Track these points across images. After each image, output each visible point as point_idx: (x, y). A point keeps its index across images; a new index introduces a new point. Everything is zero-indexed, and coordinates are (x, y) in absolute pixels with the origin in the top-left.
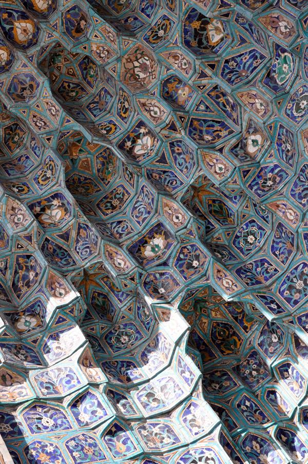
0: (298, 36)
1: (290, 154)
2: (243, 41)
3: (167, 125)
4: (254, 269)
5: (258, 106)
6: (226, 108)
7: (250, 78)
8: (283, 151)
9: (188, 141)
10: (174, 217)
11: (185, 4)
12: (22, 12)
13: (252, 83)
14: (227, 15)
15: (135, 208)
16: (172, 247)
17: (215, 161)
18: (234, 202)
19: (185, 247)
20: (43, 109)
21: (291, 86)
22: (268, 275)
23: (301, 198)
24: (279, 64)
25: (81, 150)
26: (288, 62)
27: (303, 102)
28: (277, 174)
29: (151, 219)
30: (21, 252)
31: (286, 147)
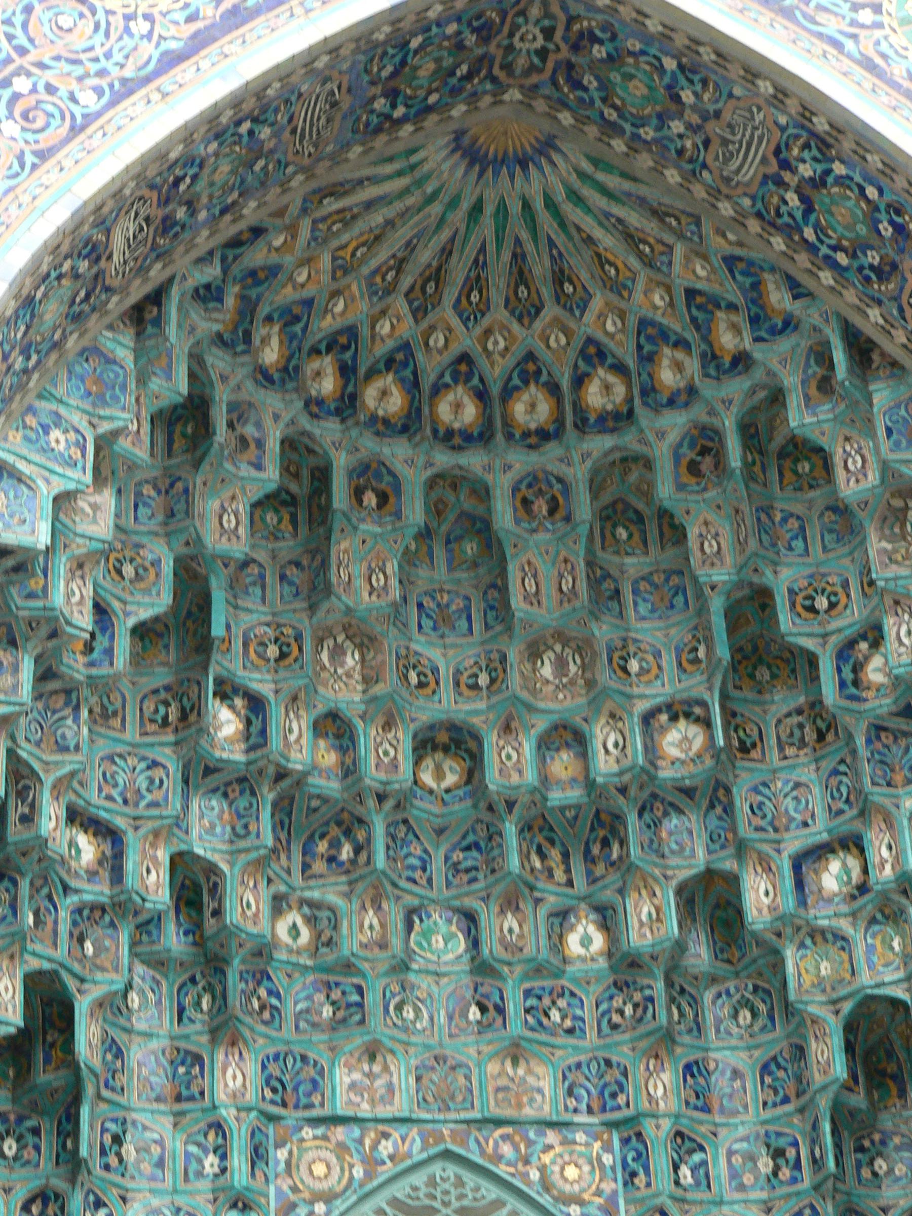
0: (509, 964)
1: (316, 1019)
2: (440, 832)
7: (403, 884)
9: (266, 815)
13: (396, 892)
14: (490, 808)
19: (104, 910)
30: (19, 630)
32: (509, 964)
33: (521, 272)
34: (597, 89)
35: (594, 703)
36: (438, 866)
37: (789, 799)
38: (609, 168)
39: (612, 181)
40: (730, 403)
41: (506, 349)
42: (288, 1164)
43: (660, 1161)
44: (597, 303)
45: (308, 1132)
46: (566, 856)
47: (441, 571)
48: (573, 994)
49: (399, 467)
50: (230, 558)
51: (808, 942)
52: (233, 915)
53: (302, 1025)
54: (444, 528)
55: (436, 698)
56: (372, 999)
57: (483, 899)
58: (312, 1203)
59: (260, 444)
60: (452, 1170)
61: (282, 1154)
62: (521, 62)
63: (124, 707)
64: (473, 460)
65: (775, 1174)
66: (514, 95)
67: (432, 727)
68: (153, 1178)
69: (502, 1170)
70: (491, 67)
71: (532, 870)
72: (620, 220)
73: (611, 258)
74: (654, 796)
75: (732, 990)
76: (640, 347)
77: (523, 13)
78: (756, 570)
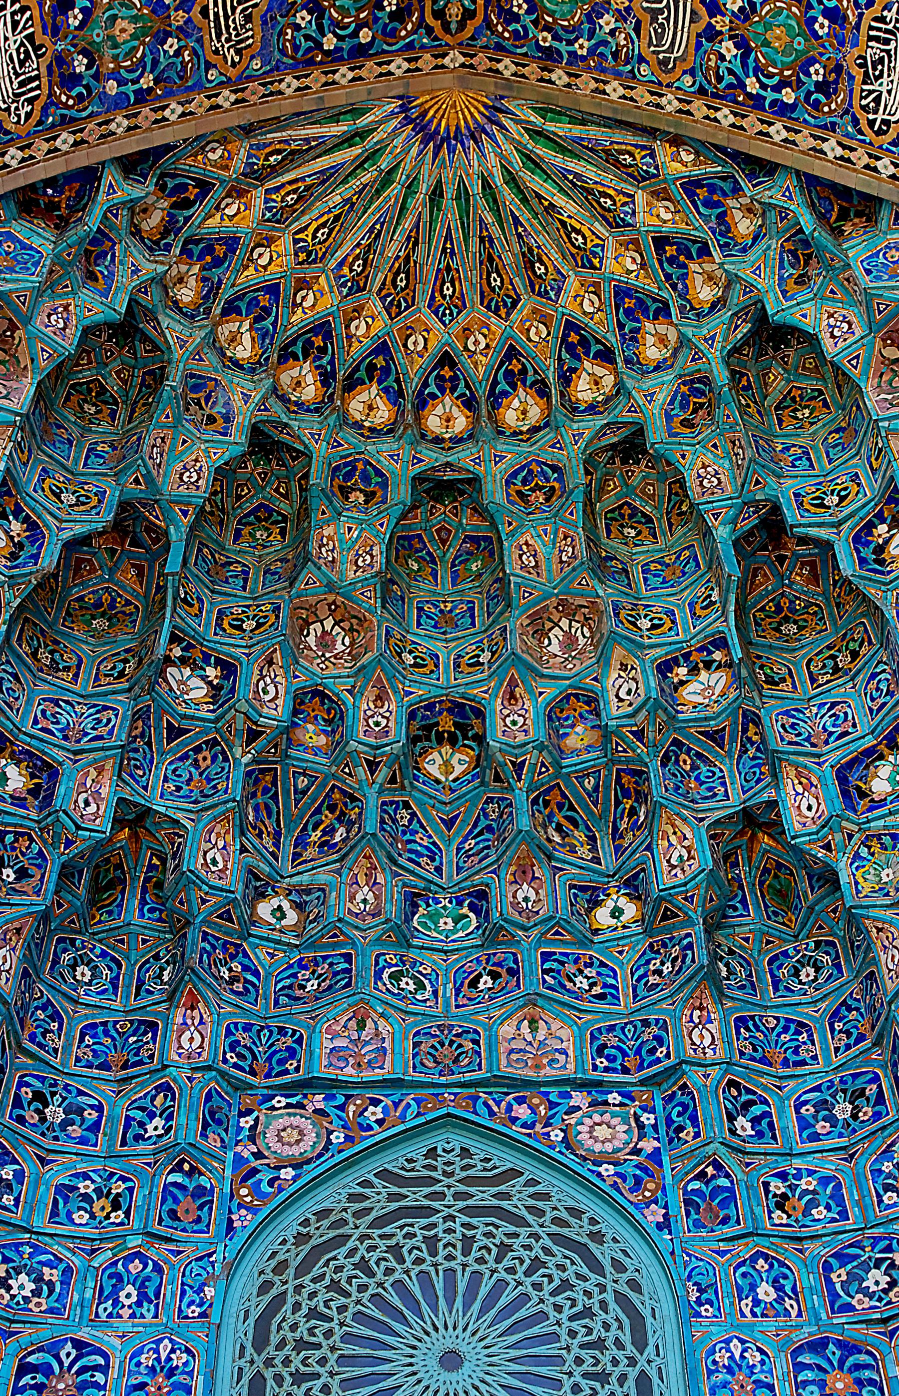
1: (299, 993)
2: (449, 823)
3: (255, 723)
4: (36, 1004)
5: (359, 897)
6: (314, 830)
7: (401, 861)
8: (294, 975)
9: (237, 776)
10: (84, 795)
11: (485, 692)
12: (333, 373)
14: (497, 778)
15: (56, 703)
16: (22, 812)
17: (221, 844)
18: (141, 910)
19: (31, 840)
20: (182, 453)
21: (422, 948)
22: (40, 1038)
23: (233, 1047)
24: (444, 908)
25: (113, 552)
26: (459, 926)
27: (411, 982)
28: (246, 981)
29: (55, 746)
31: (308, 980)
32: (526, 929)
33: (491, 259)
34: (528, 12)
35: (603, 660)
36: (449, 857)
37: (826, 718)
39: (561, 128)
40: (713, 338)
41: (487, 346)
42: (253, 1128)
43: (711, 1110)
44: (572, 284)
45: (280, 1101)
46: (592, 839)
47: (445, 585)
48: (603, 964)
49: (385, 464)
50: (189, 504)
51: (864, 852)
52: (193, 862)
53: (283, 1000)
54: (450, 556)
55: (434, 676)
56: (363, 964)
57: (494, 872)
58: (278, 1168)
59: (228, 419)
60: (457, 1139)
61: (246, 1122)
63: (79, 667)
64: (463, 456)
65: (855, 1117)
66: (454, 59)
67: (430, 707)
68: (83, 1141)
69: (516, 1131)
71: (549, 840)
72: (576, 175)
73: (578, 226)
74: (676, 743)
75: (791, 952)
76: (621, 326)
78: (758, 482)
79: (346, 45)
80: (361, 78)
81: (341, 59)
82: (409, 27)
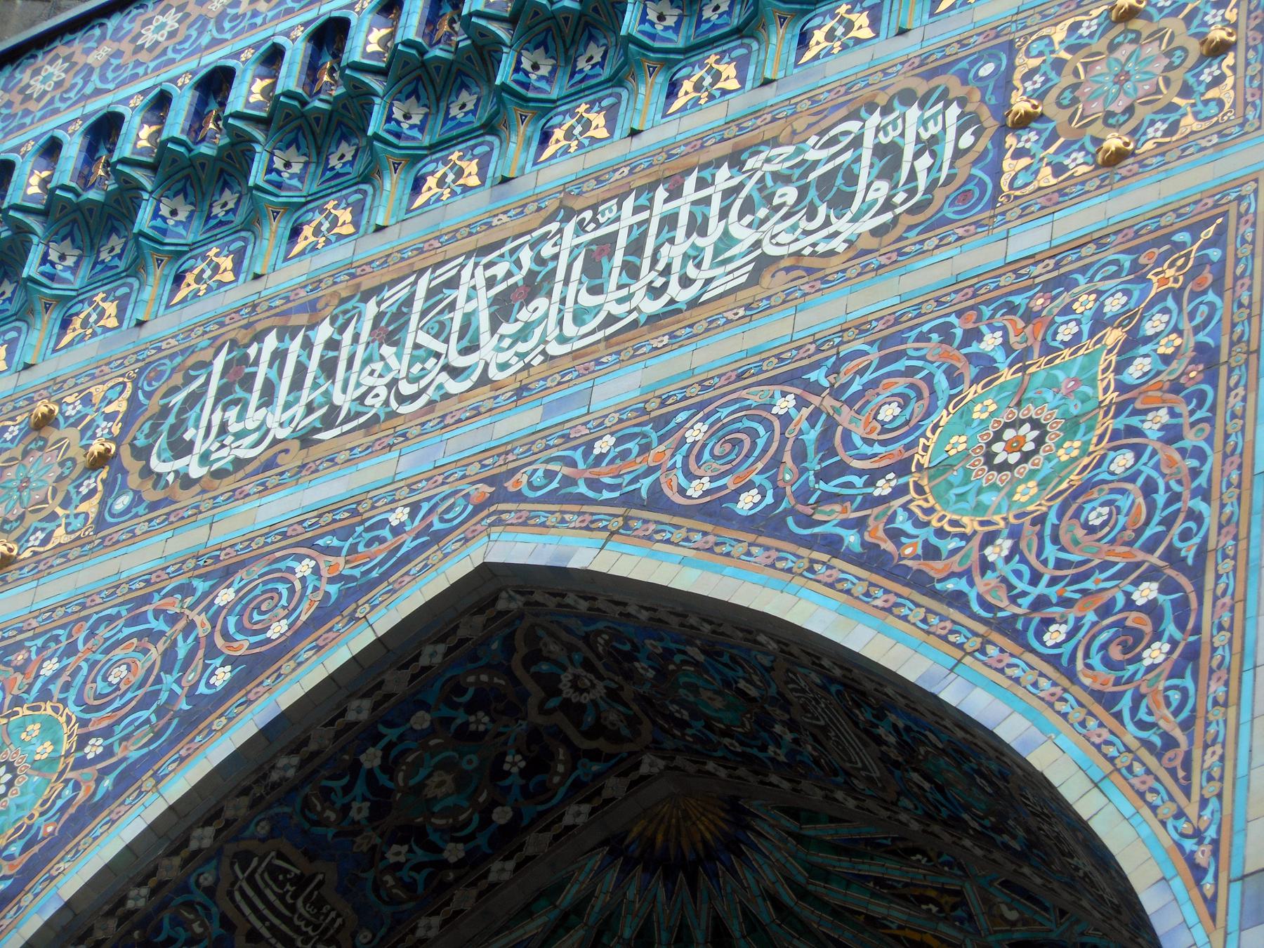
38: (813, 817)
39: (825, 831)
62: (612, 717)
66: (650, 764)
70: (567, 741)
72: (879, 881)
77: (535, 656)
79: (482, 840)
80: (529, 859)
81: (486, 858)
82: (561, 768)
